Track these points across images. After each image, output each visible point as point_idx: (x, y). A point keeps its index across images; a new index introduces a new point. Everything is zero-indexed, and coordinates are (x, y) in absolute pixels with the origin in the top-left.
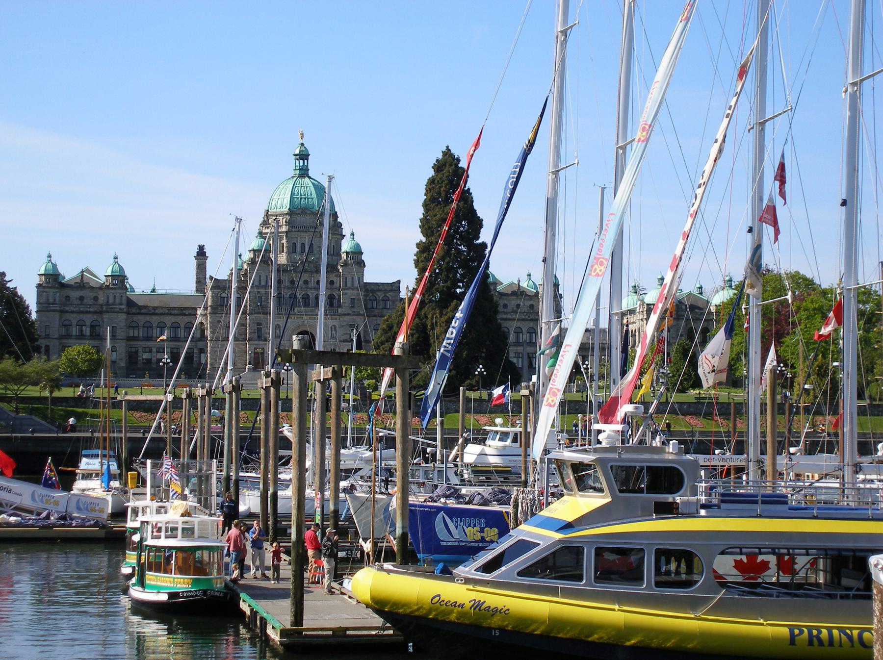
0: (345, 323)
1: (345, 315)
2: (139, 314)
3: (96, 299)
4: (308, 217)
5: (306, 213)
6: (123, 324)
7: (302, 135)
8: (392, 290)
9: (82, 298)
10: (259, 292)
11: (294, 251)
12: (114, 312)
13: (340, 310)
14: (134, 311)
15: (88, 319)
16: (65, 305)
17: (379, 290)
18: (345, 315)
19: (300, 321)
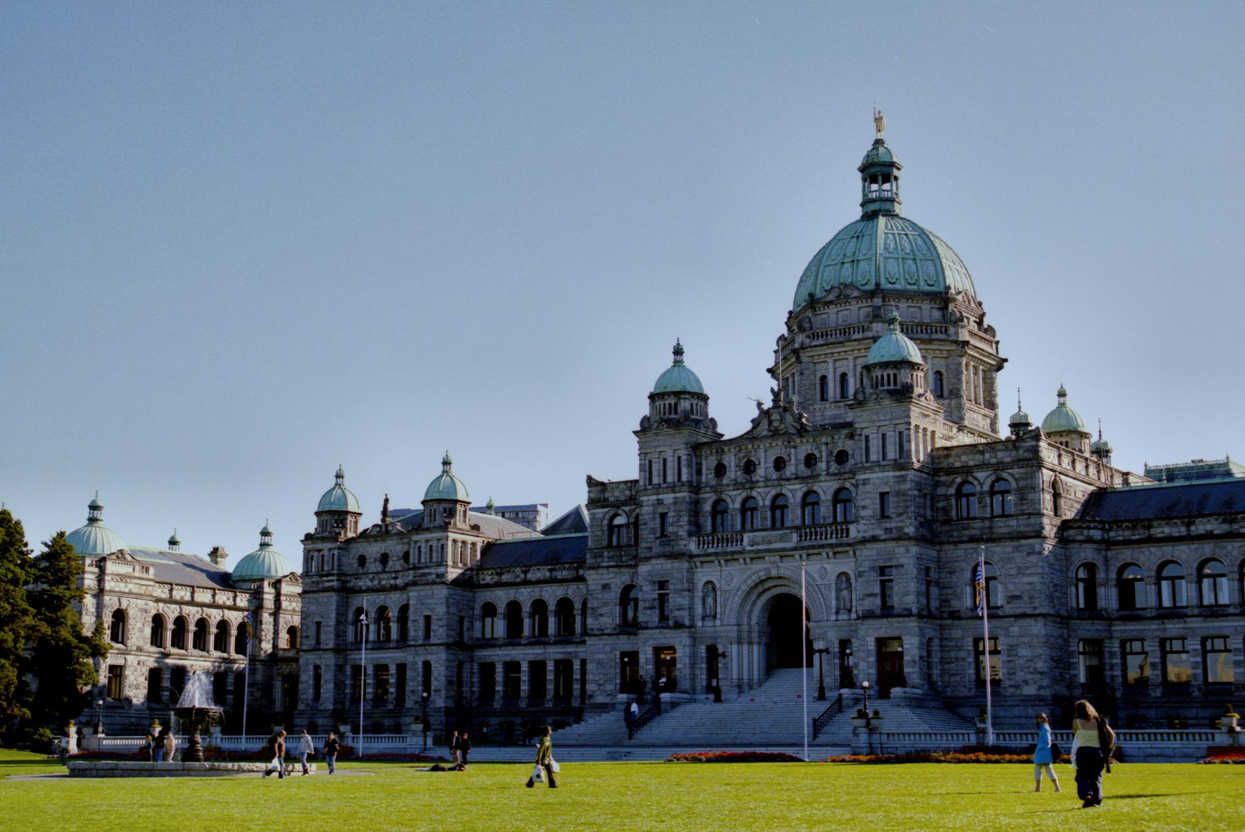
0: (865, 566)
1: (864, 541)
2: (499, 585)
3: (406, 556)
4: (854, 307)
5: (847, 297)
6: (441, 610)
7: (878, 120)
8: (1018, 462)
9: (384, 558)
10: (660, 502)
11: (823, 398)
12: (427, 584)
13: (852, 528)
14: (488, 579)
15: (393, 601)
16: (357, 576)
17: (982, 466)
18: (864, 541)
19: (758, 569)
